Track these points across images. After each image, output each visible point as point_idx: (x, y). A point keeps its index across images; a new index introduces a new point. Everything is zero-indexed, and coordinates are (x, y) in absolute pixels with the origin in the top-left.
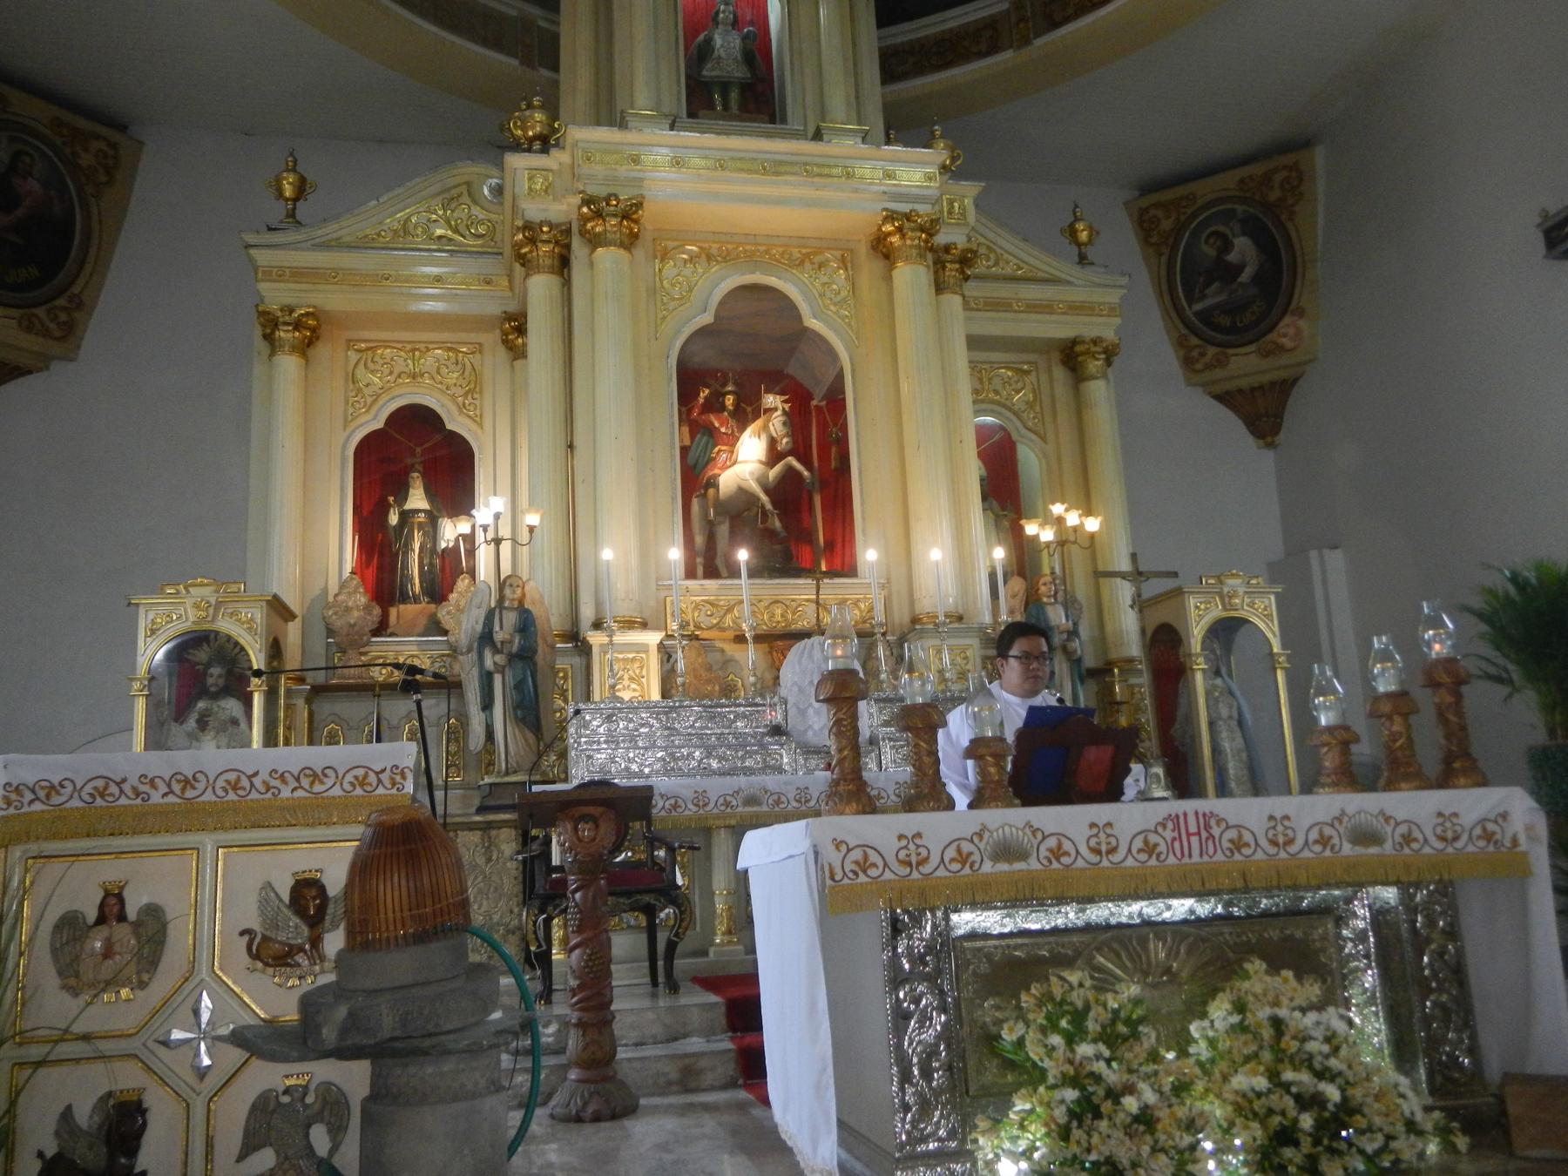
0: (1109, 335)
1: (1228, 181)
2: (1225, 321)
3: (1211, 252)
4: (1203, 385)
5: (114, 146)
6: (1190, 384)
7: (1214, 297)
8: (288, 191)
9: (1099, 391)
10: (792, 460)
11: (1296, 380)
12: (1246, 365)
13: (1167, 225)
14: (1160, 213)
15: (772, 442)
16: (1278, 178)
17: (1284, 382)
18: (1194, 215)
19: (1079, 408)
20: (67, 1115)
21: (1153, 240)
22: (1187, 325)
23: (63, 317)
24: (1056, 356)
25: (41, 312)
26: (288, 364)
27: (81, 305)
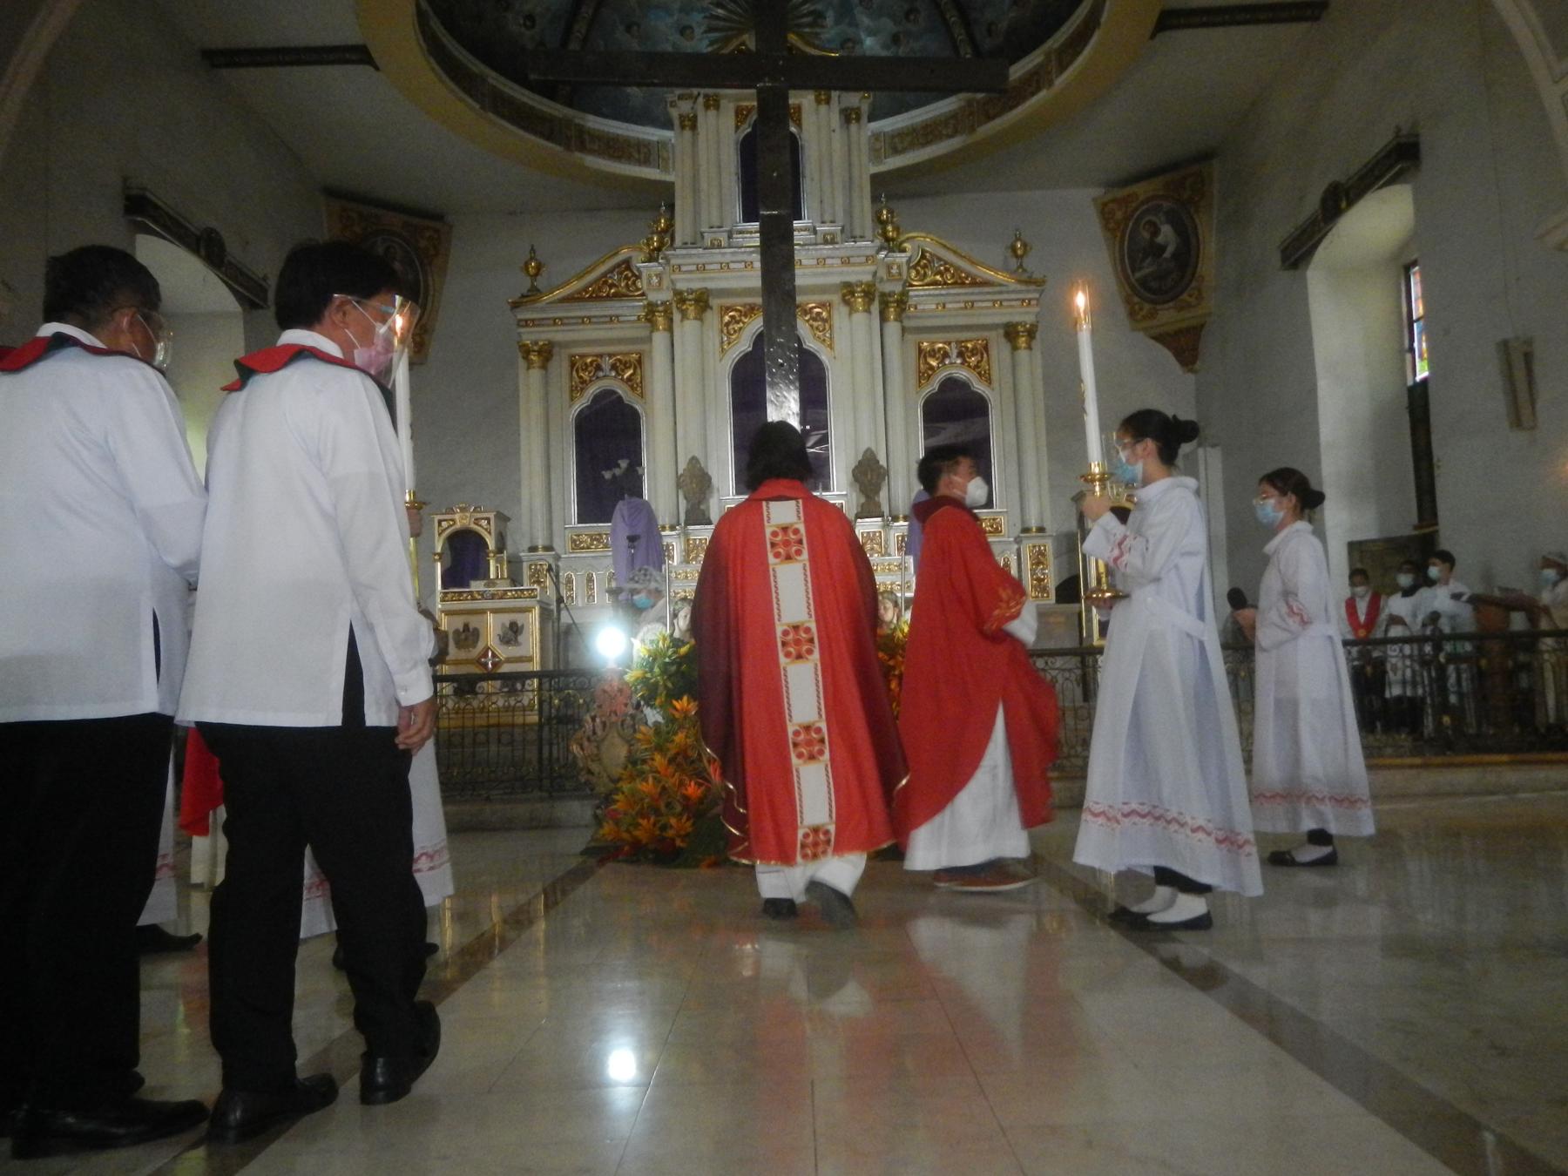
0: (1029, 319)
2: (1154, 285)
3: (1146, 235)
4: (1145, 330)
5: (437, 231)
6: (1133, 330)
8: (532, 271)
9: (1023, 354)
11: (1202, 326)
12: (1168, 317)
13: (1119, 215)
18: (1136, 209)
19: (1014, 367)
22: (1132, 287)
24: (1001, 332)
26: (536, 374)
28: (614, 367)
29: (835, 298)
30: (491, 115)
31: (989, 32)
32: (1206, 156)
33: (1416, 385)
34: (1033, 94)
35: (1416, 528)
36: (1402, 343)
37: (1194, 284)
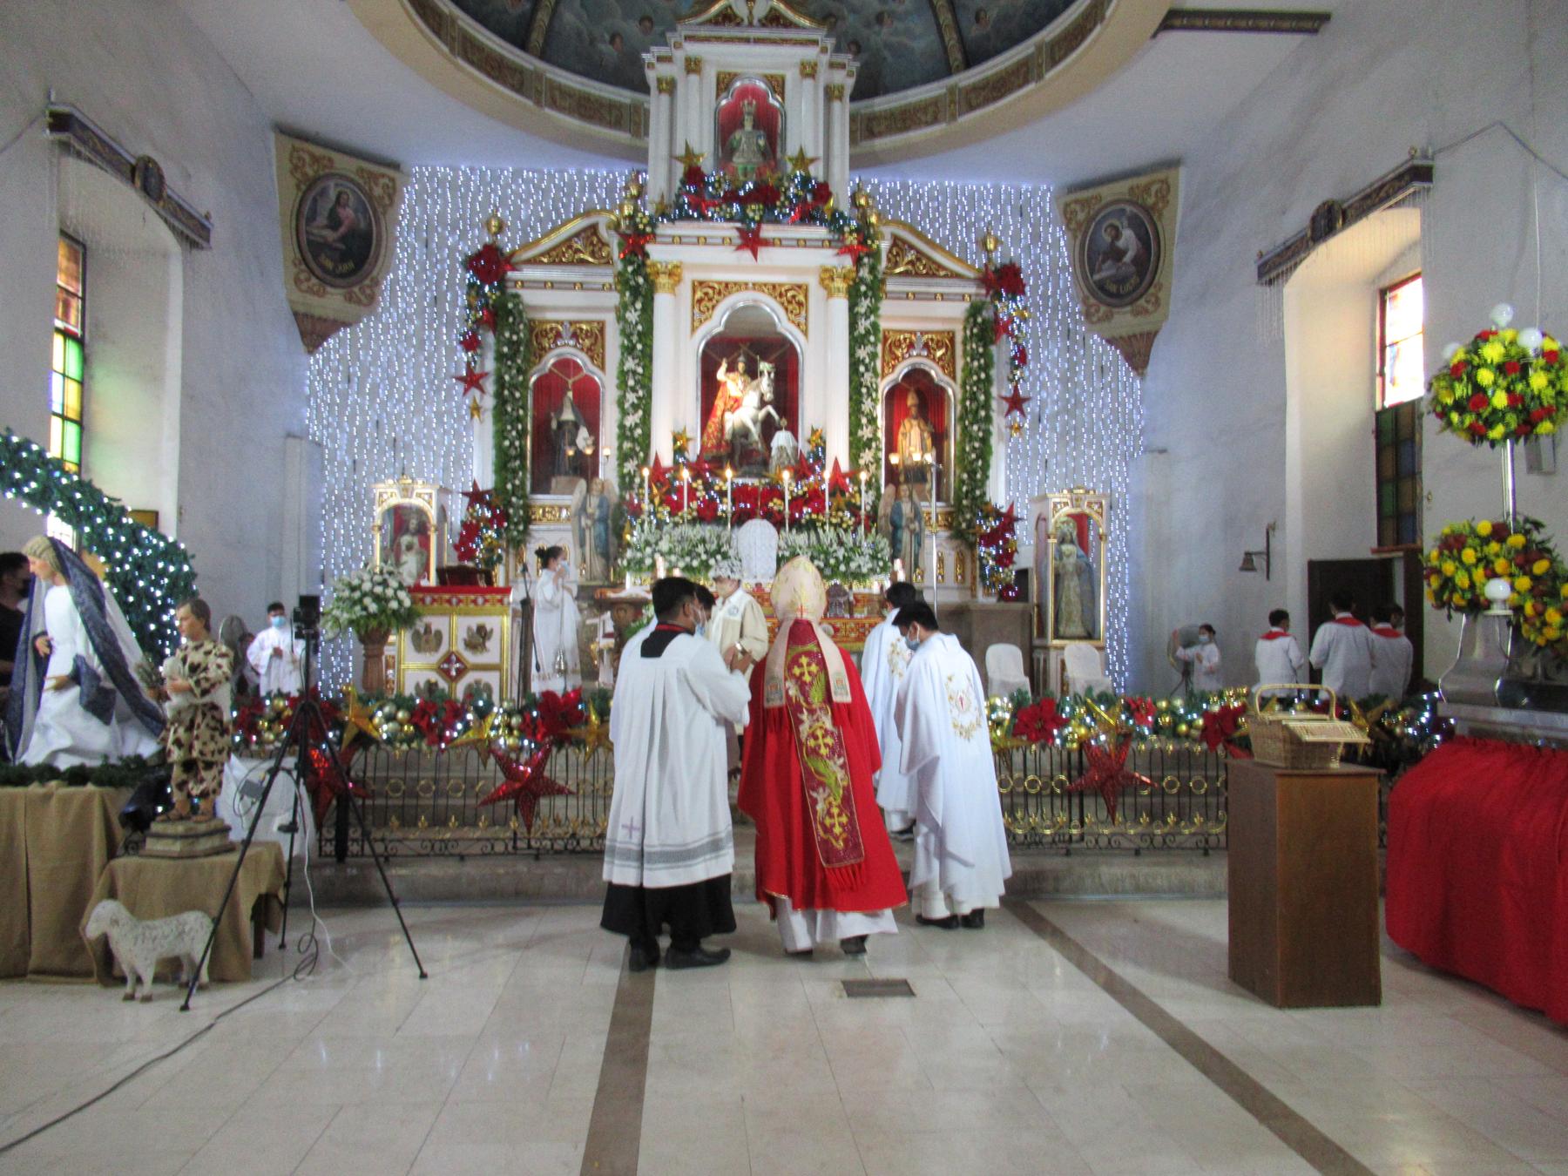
1: (1122, 188)
2: (1113, 288)
3: (1108, 239)
5: (392, 180)
7: (1107, 271)
10: (770, 408)
11: (1156, 333)
12: (1125, 321)
13: (1081, 216)
14: (1078, 208)
15: (762, 395)
16: (1154, 188)
17: (1149, 334)
20: (418, 685)
21: (1073, 226)
23: (368, 291)
25: (356, 289)
27: (376, 283)
28: (575, 336)
29: (812, 281)
30: (460, 61)
31: (978, 19)
32: (1173, 164)
33: (1384, 410)
34: (1020, 86)
35: (1374, 551)
36: (1373, 368)
37: (1152, 290)
